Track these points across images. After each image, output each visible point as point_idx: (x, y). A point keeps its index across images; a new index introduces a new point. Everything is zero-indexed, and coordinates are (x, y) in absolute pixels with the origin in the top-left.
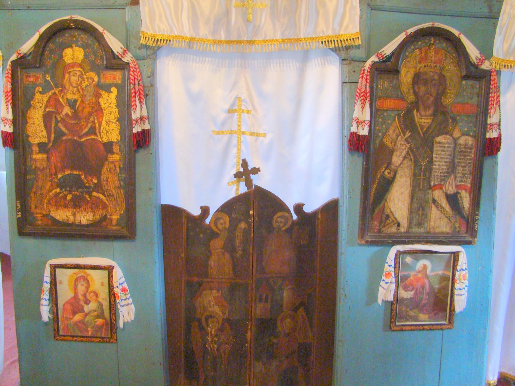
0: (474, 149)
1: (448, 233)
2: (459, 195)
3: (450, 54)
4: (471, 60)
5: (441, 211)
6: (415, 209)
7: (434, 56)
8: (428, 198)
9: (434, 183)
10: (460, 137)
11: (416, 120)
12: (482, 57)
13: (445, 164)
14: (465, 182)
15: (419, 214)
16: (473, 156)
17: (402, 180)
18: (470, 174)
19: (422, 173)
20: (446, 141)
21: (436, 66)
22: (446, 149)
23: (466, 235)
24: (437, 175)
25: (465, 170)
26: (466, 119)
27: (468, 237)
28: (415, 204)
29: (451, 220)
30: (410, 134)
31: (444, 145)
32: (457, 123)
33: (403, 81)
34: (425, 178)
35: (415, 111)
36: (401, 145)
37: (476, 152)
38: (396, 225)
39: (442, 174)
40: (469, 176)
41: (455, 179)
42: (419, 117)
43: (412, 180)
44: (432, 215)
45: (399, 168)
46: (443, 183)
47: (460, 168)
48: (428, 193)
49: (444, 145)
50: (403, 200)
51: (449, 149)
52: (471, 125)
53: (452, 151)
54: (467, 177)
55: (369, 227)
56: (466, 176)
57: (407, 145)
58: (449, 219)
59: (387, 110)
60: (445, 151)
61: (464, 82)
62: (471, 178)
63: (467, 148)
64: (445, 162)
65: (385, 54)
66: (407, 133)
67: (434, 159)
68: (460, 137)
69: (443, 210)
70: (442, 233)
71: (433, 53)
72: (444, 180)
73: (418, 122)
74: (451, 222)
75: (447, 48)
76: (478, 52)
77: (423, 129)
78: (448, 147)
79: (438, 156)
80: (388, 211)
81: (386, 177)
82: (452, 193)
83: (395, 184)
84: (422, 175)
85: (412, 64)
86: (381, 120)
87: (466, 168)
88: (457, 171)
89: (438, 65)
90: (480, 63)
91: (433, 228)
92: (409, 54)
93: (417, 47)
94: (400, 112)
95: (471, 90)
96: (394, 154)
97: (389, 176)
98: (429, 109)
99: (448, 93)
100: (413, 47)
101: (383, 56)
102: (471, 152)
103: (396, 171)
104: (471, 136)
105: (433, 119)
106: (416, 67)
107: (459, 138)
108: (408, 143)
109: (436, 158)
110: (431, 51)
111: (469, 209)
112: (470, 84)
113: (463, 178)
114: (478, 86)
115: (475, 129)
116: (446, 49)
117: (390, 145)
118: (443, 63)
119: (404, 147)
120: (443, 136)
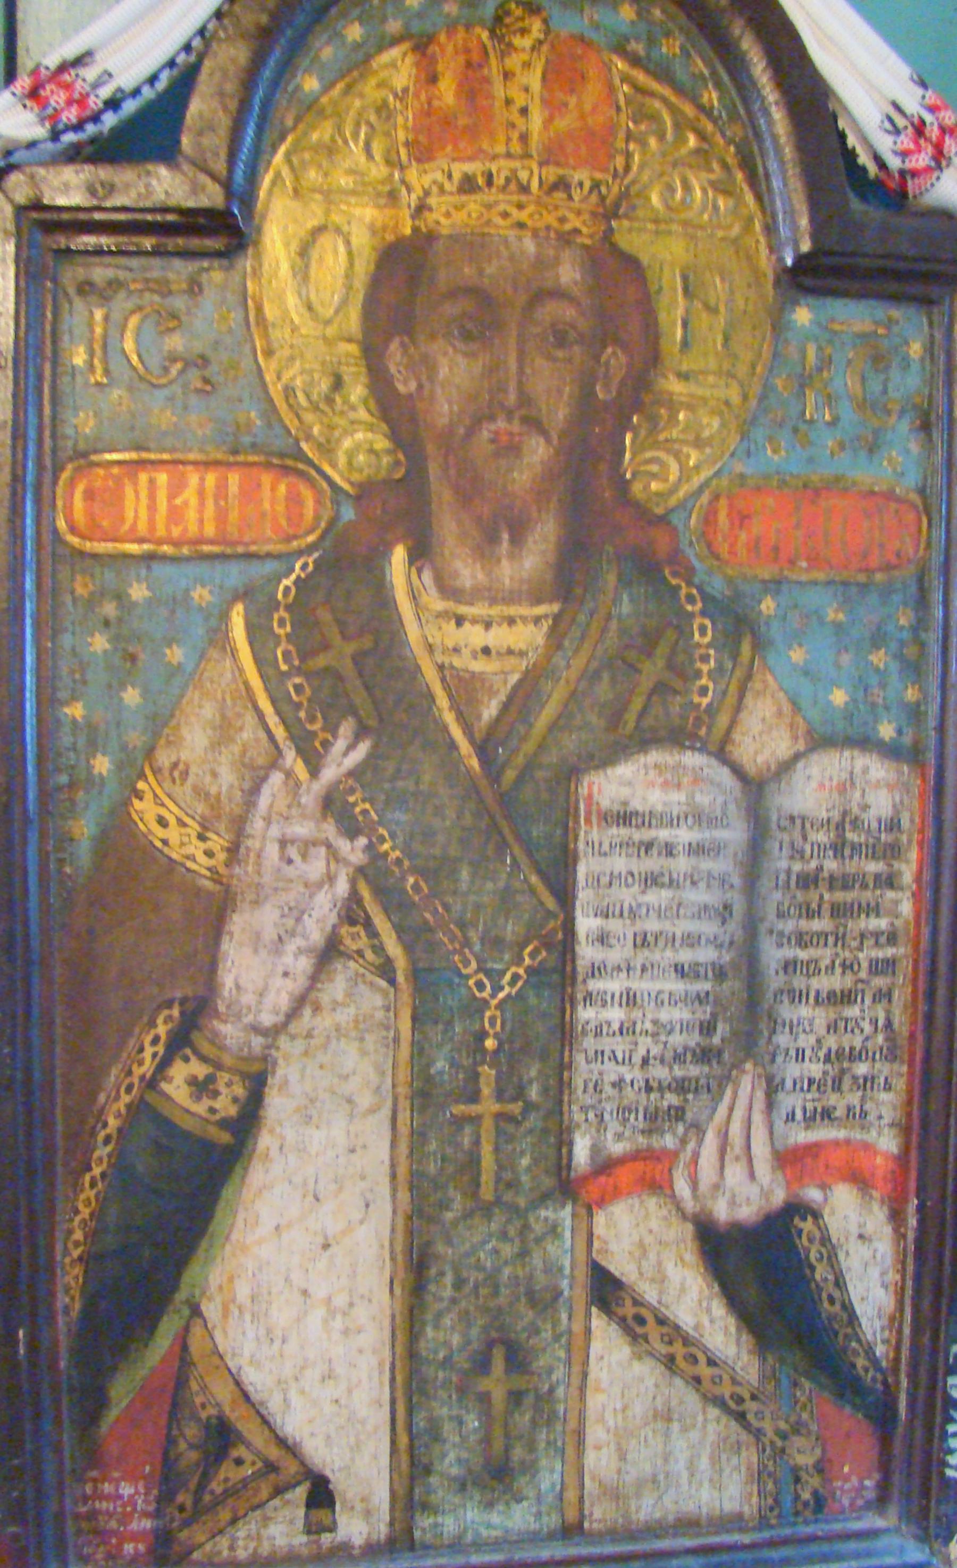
0: (913, 855)
1: (736, 1521)
2: (808, 1225)
3: (680, 90)
4: (851, 141)
5: (670, 1362)
6: (447, 1362)
7: (546, 102)
8: (553, 1269)
9: (595, 1150)
10: (797, 757)
11: (413, 632)
12: (933, 109)
13: (677, 986)
14: (857, 1116)
15: (485, 1399)
16: (906, 908)
17: (316, 1137)
18: (891, 1055)
19: (487, 1072)
20: (677, 797)
21: (562, 185)
22: (682, 864)
23: (880, 1523)
24: (618, 1084)
25: (850, 1026)
26: (833, 614)
27: (898, 1530)
28: (447, 1321)
29: (755, 1423)
30: (363, 748)
31: (664, 834)
32: (760, 645)
33: (285, 313)
34: (516, 1108)
35: (399, 554)
36: (293, 852)
37: (927, 876)
38: (300, 1493)
39: (659, 1073)
40: (883, 1069)
41: (770, 1105)
42: (437, 604)
43: (404, 1129)
44: (594, 1401)
45: (283, 1041)
46: (669, 1141)
47: (804, 1011)
48: (554, 1230)
49: (664, 834)
50: (340, 1301)
51: (707, 864)
52: (878, 658)
53: (736, 880)
54: (867, 1082)
55: (70, 1527)
56: (862, 1069)
57: (343, 845)
58: (741, 1417)
59: (151, 557)
60: (672, 884)
61: (802, 316)
62: (900, 1084)
63: (856, 848)
64: (680, 971)
65: (96, 85)
66: (340, 745)
67: (587, 953)
68: (797, 757)
69: (678, 1349)
70: (688, 1524)
71: (534, 80)
72: (678, 1113)
73: (430, 648)
74: (758, 1434)
75: (651, 42)
76: (905, 71)
77: (473, 701)
78: (697, 850)
79: (614, 925)
80: (223, 1393)
81: (187, 1124)
82: (747, 1213)
83: (257, 1175)
84: (486, 1091)
85: (351, 172)
86: (100, 643)
87: (853, 1011)
88: (782, 1039)
89: (581, 175)
90: (923, 160)
91: (614, 1494)
92: (326, 89)
93: (394, 26)
94: (269, 567)
95: (863, 379)
96: (238, 922)
97: (200, 1108)
98: (517, 540)
99: (673, 407)
100: (355, 32)
101: (82, 102)
102: (889, 881)
103: (256, 1067)
104: (890, 752)
105: (557, 618)
106: (393, 196)
107: (786, 767)
108: (352, 833)
109: (603, 939)
110: (514, 62)
111: (894, 1321)
112: (857, 328)
113: (837, 1086)
114: (916, 349)
115: (911, 694)
116: (638, 47)
117: (196, 848)
118: (620, 161)
119: (316, 867)
120: (654, 756)
